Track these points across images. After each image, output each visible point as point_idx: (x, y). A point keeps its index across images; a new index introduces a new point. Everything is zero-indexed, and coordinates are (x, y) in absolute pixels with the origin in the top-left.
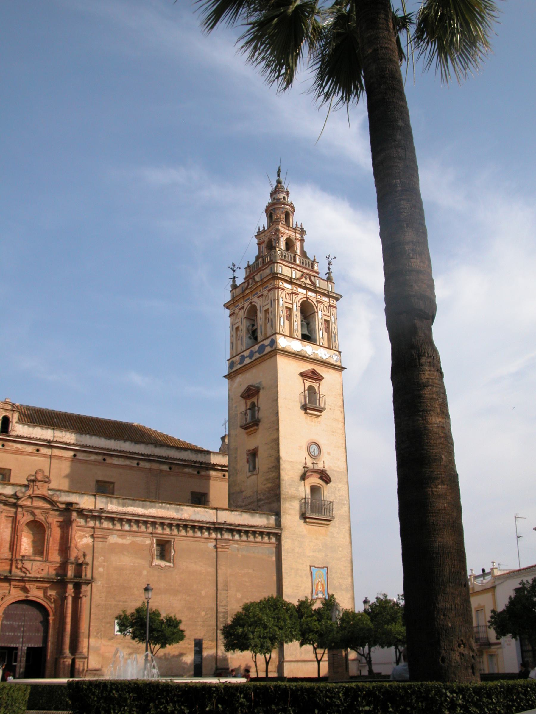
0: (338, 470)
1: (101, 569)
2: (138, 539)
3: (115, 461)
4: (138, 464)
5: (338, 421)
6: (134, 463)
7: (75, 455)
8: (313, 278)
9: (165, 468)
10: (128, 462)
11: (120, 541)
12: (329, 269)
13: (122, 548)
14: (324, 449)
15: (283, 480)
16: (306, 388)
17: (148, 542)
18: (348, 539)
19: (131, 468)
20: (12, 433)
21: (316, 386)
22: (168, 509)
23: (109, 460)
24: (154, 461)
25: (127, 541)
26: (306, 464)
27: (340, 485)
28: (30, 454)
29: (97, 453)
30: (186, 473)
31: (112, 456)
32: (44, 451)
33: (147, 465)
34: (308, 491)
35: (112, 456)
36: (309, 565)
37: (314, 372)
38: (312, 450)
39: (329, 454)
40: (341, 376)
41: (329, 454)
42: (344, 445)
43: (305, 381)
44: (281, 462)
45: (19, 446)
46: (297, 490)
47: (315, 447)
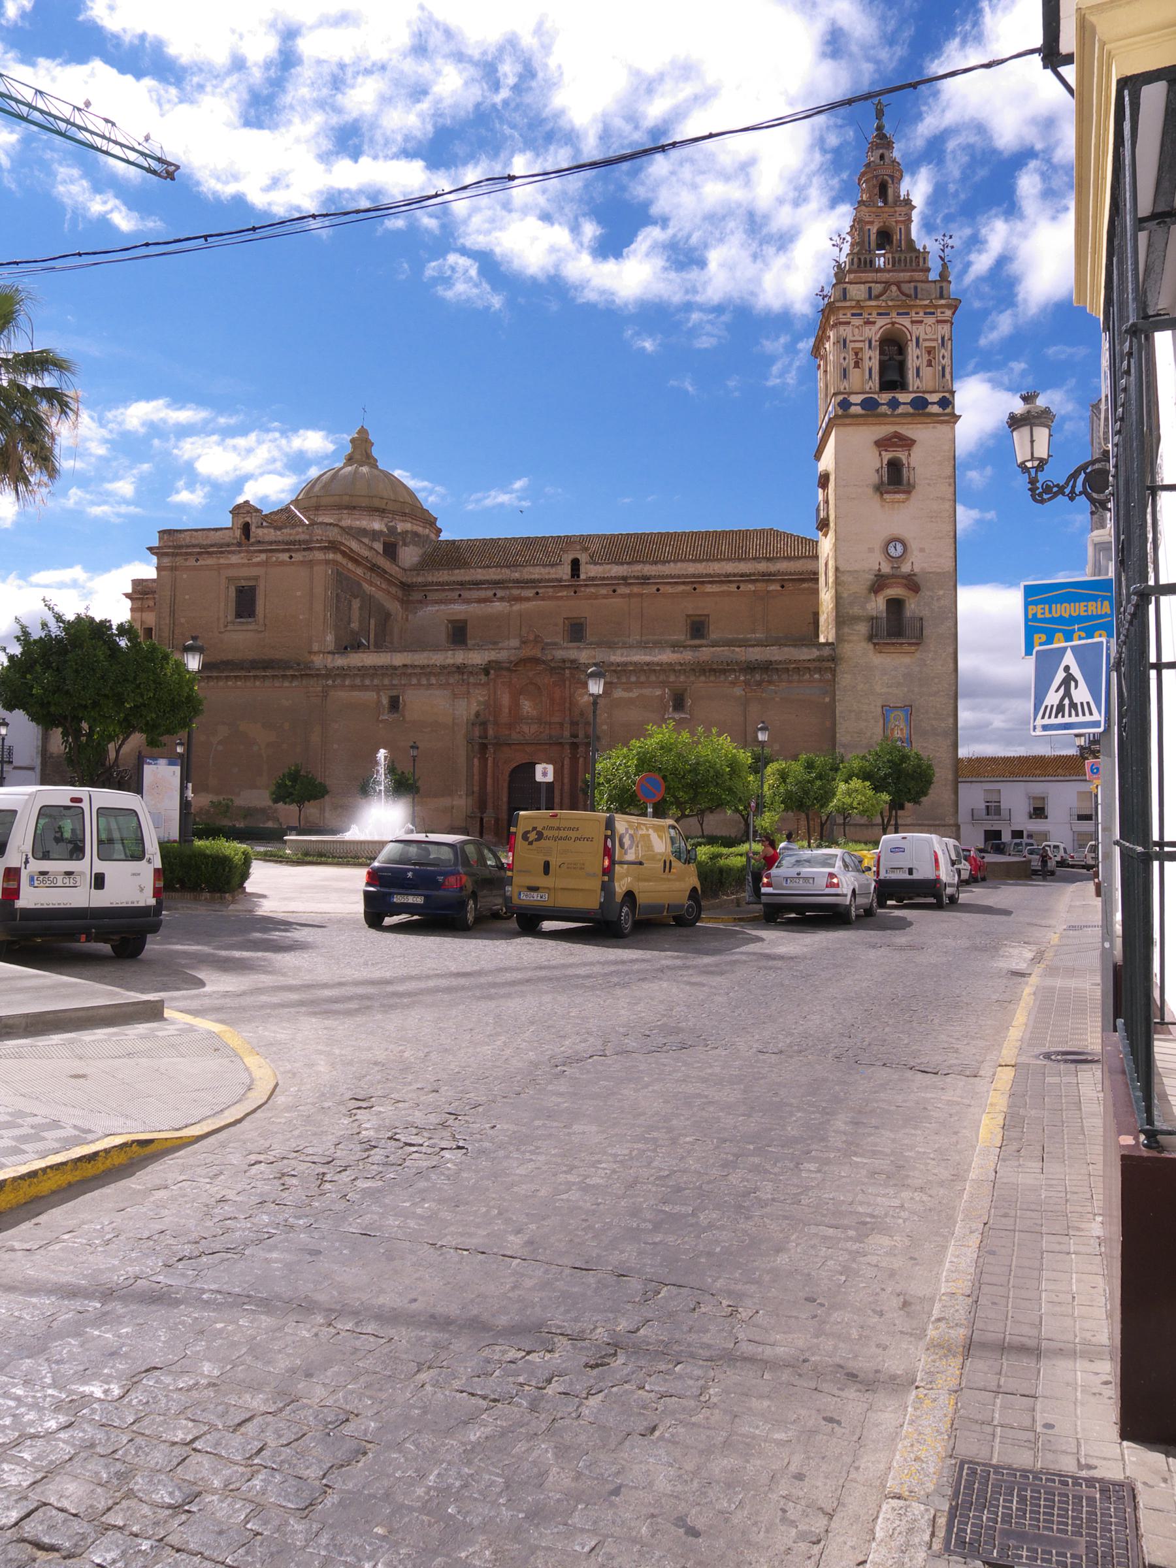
1: (605, 727)
2: (647, 691)
3: (709, 588)
4: (738, 588)
5: (943, 499)
6: (733, 587)
7: (658, 590)
8: (905, 287)
9: (775, 587)
10: (725, 588)
11: (626, 695)
13: (631, 701)
14: (914, 545)
16: (885, 462)
17: (658, 692)
19: (730, 594)
20: (582, 576)
21: (902, 455)
24: (757, 580)
25: (634, 694)
26: (879, 570)
27: (941, 593)
28: (605, 597)
29: (684, 583)
30: (804, 589)
31: (703, 583)
32: (623, 590)
33: (751, 587)
35: (703, 583)
36: (879, 704)
37: (897, 435)
38: (892, 551)
39: (922, 550)
40: (953, 429)
41: (922, 550)
42: (952, 534)
43: (883, 453)
45: (592, 590)
47: (899, 547)
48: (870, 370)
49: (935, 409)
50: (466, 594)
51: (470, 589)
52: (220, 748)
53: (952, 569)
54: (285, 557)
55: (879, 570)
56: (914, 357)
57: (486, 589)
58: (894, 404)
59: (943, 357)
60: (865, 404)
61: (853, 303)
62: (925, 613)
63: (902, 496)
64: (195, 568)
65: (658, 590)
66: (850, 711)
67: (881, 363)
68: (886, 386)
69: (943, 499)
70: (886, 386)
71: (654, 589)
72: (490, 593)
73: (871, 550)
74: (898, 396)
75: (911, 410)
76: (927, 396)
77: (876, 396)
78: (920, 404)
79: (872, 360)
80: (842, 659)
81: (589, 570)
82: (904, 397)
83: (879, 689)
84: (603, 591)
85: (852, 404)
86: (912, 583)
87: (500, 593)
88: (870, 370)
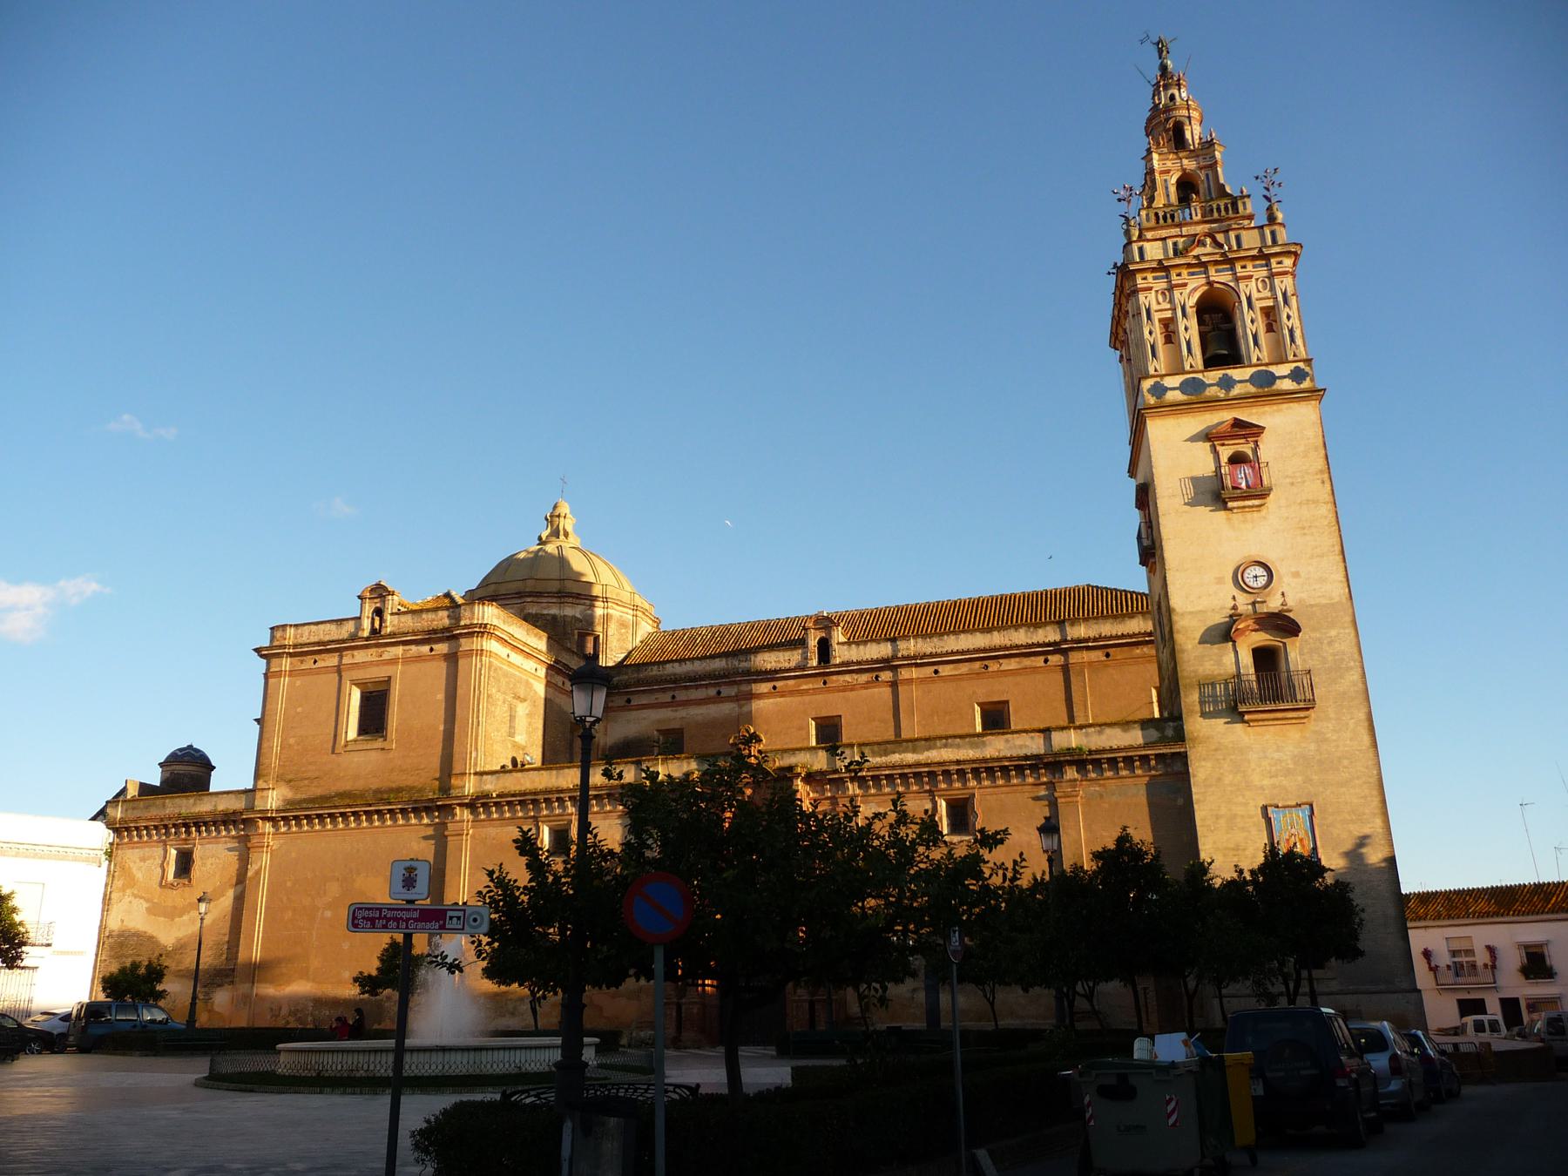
0: (1324, 601)
4: (1046, 661)
5: (1316, 502)
6: (1039, 661)
7: (936, 672)
8: (1220, 238)
10: (1027, 662)
12: (1269, 199)
15: (1183, 651)
16: (1224, 459)
18: (1366, 739)
19: (1035, 669)
20: (833, 662)
21: (1247, 449)
22: (958, 747)
23: (993, 666)
26: (1235, 608)
27: (1333, 633)
28: (866, 685)
34: (1247, 659)
37: (1238, 423)
39: (1296, 575)
41: (1296, 575)
42: (1338, 548)
44: (1175, 618)
45: (848, 678)
46: (1219, 663)
47: (1260, 571)
48: (1188, 343)
49: (1287, 385)
50: (682, 695)
51: (686, 688)
52: (328, 914)
53: (1344, 599)
54: (425, 649)
55: (1235, 608)
56: (1250, 323)
57: (706, 686)
58: (1227, 383)
59: (1289, 317)
60: (1183, 387)
61: (1154, 265)
62: (1313, 663)
63: (1256, 502)
64: (309, 672)
65: (936, 672)
66: (1218, 817)
67: (1202, 336)
68: (1210, 362)
69: (1316, 502)
70: (1210, 362)
71: (929, 671)
72: (712, 692)
73: (1220, 581)
74: (1229, 372)
75: (1252, 389)
76: (1272, 369)
77: (1200, 376)
78: (1265, 379)
79: (1189, 330)
80: (1194, 740)
81: (840, 654)
82: (1236, 373)
83: (1256, 779)
84: (864, 678)
85: (1167, 389)
86: (1284, 624)
87: (726, 691)
88: (1188, 343)
